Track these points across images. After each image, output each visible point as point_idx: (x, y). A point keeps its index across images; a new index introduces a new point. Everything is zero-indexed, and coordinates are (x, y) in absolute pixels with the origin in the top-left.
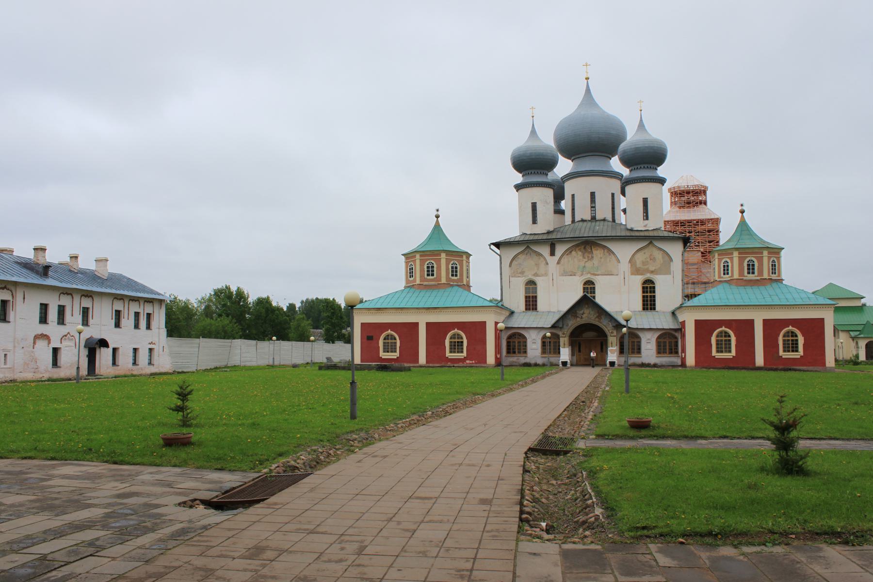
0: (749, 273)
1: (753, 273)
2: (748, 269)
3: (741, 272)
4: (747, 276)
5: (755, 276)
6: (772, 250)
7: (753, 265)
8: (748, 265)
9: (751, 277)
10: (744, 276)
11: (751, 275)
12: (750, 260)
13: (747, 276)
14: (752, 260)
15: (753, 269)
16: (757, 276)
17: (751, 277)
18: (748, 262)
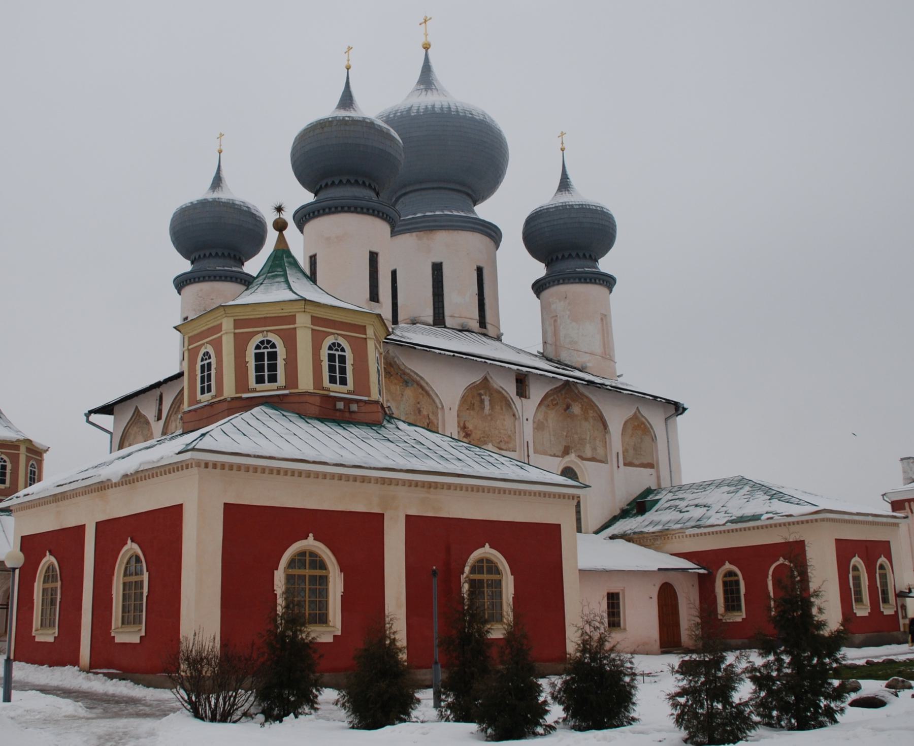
0: (260, 380)
1: (273, 379)
2: (259, 368)
3: (241, 382)
4: (255, 391)
5: (278, 389)
6: (321, 313)
7: (273, 356)
8: (259, 357)
9: (267, 389)
10: (249, 391)
11: (267, 385)
12: (262, 342)
13: (255, 391)
14: (269, 342)
15: (273, 368)
16: (285, 388)
17: (267, 389)
18: (258, 347)
